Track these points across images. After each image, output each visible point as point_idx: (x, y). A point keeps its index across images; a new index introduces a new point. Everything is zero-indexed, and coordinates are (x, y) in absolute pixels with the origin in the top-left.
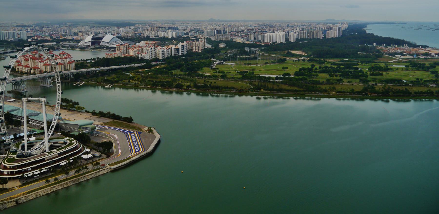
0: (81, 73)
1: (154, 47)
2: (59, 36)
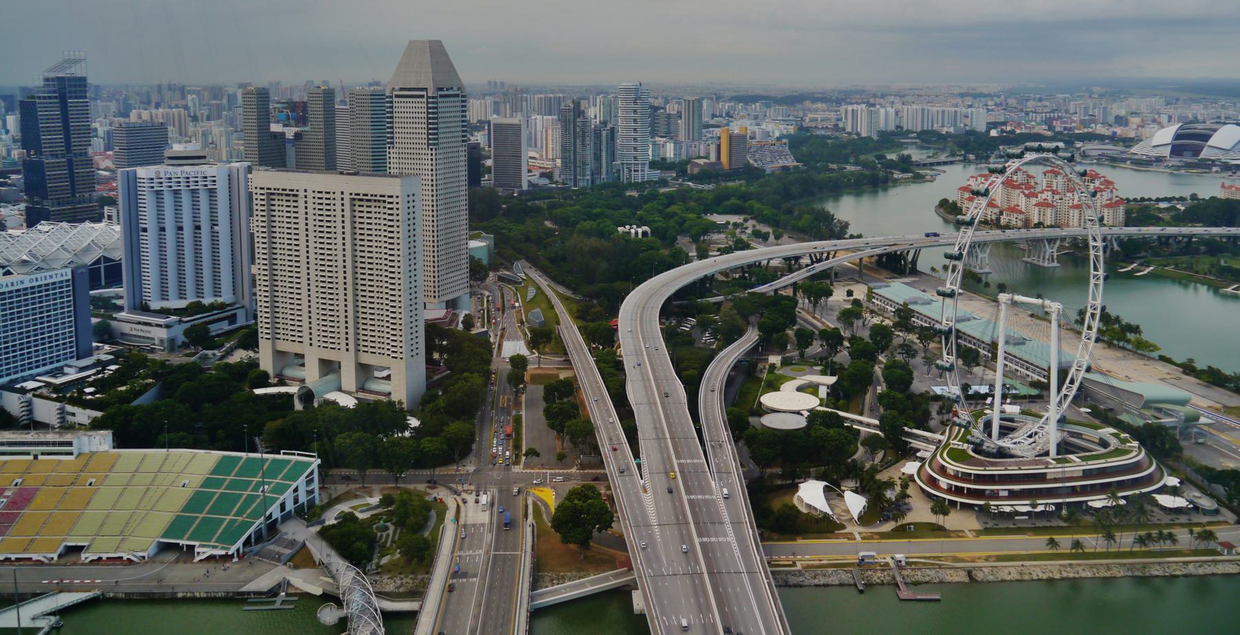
0: (1143, 238)
2: (1073, 125)
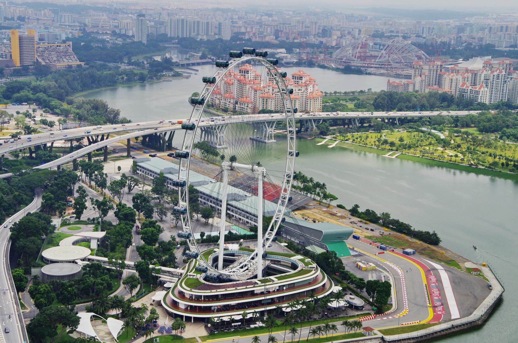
1: (504, 73)
